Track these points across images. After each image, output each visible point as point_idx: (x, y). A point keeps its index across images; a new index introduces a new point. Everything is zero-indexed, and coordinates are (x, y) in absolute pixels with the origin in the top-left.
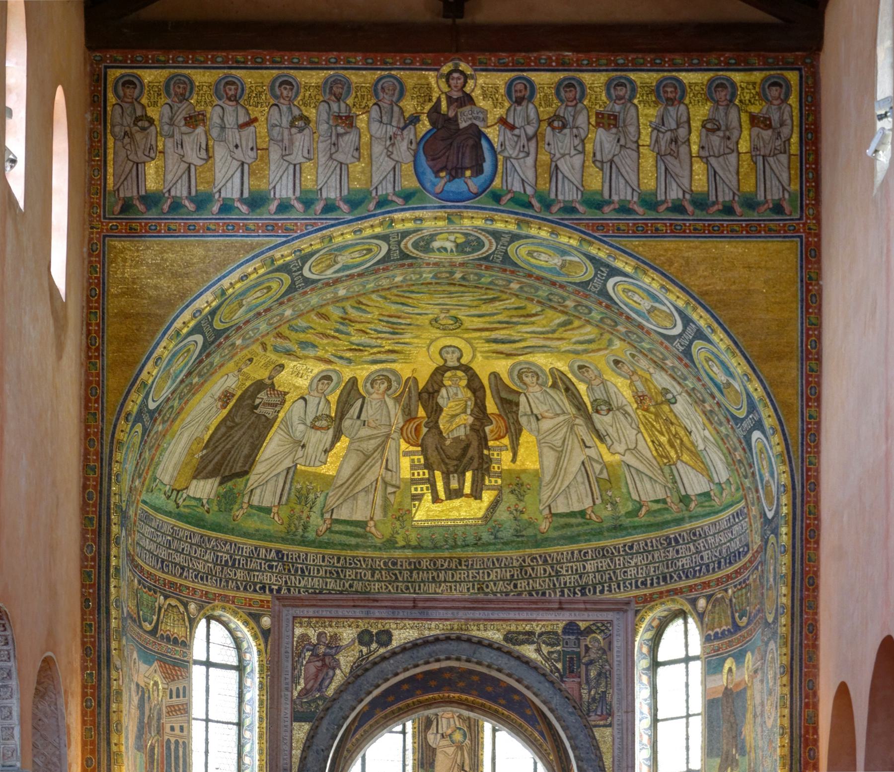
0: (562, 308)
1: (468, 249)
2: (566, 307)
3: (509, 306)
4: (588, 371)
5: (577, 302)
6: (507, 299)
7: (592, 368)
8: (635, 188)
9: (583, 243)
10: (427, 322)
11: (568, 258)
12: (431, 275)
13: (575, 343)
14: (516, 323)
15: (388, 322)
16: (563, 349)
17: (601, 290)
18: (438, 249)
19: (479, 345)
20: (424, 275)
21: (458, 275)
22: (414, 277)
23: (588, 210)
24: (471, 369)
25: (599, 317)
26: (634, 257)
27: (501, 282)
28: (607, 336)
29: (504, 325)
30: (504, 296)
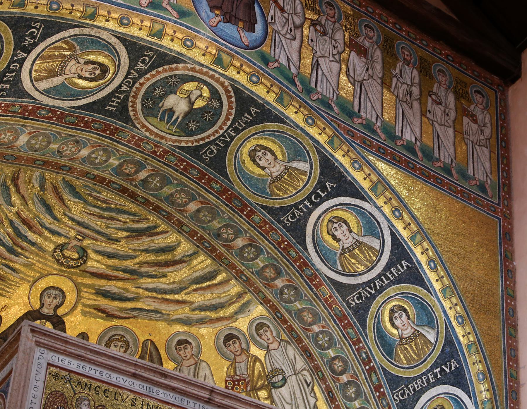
0: (222, 250)
1: (193, 126)
2: (228, 247)
3: (154, 246)
4: (185, 349)
5: (251, 239)
6: (162, 233)
7: (194, 344)
8: (379, 115)
9: (335, 139)
10: (50, 247)
11: (296, 164)
12: (117, 163)
13: (193, 310)
14: (141, 275)
15: (16, 230)
16: (175, 317)
17: (299, 220)
18: (165, 112)
19: (86, 295)
20: (111, 160)
21: (143, 175)
22: (101, 156)
23: (341, 113)
24: (64, 323)
25: (262, 265)
26: (377, 173)
27: (181, 198)
28: (248, 297)
29: (128, 276)
30: (163, 227)
